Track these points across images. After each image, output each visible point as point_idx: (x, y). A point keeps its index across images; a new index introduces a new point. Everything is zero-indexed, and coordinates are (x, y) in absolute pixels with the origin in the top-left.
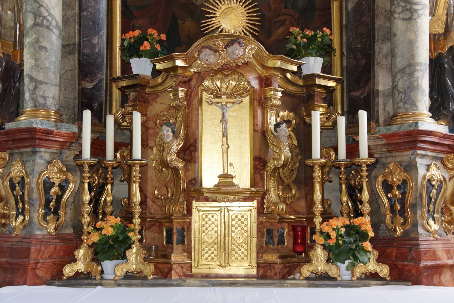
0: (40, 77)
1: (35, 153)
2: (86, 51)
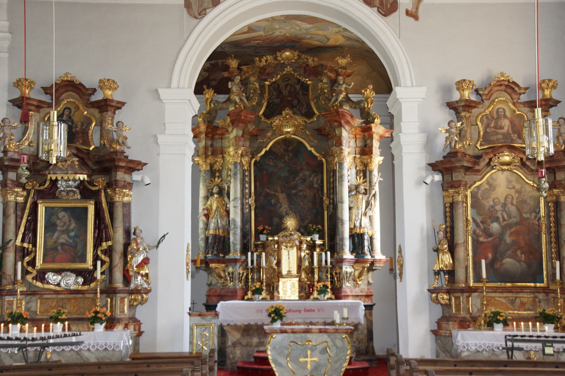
0: (235, 243)
1: (236, 265)
2: (245, 231)
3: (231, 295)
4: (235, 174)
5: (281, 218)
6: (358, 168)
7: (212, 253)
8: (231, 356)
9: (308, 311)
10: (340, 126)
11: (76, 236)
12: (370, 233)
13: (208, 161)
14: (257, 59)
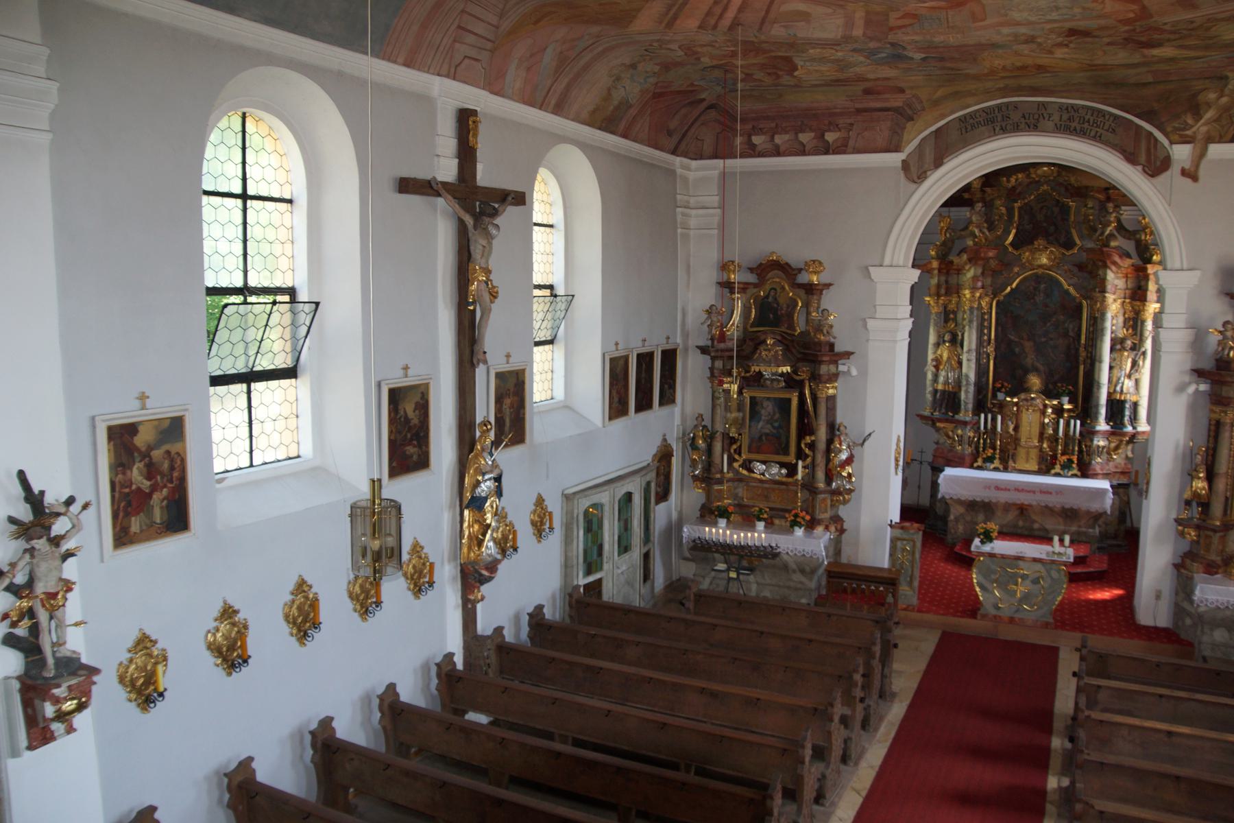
3: (958, 462)
4: (971, 321)
5: (1027, 371)
6: (1126, 316)
7: (940, 411)
8: (953, 531)
9: (1044, 493)
10: (1105, 267)
11: (780, 427)
12: (1134, 399)
13: (941, 302)
14: (1005, 179)
